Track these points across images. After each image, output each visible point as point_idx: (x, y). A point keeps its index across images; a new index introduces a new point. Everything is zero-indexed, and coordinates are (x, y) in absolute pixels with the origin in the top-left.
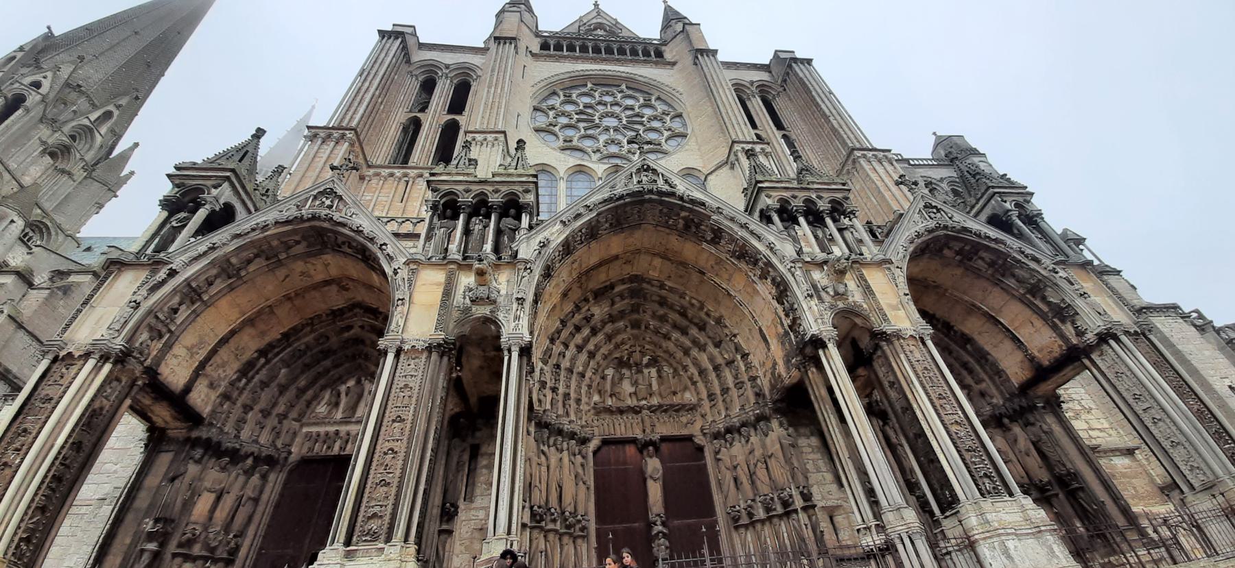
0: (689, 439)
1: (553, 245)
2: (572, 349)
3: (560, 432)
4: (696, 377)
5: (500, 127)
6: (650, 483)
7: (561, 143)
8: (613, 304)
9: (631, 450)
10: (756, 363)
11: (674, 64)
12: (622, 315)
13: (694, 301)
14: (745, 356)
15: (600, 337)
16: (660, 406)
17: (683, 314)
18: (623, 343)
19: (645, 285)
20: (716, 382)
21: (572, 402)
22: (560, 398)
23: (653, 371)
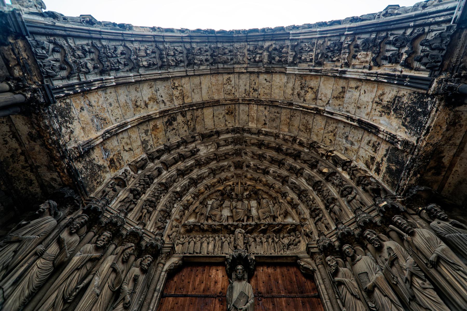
8: (219, 146)
12: (226, 156)
13: (287, 137)
15: (205, 170)
16: (257, 225)
18: (226, 179)
19: (245, 134)
20: (318, 200)
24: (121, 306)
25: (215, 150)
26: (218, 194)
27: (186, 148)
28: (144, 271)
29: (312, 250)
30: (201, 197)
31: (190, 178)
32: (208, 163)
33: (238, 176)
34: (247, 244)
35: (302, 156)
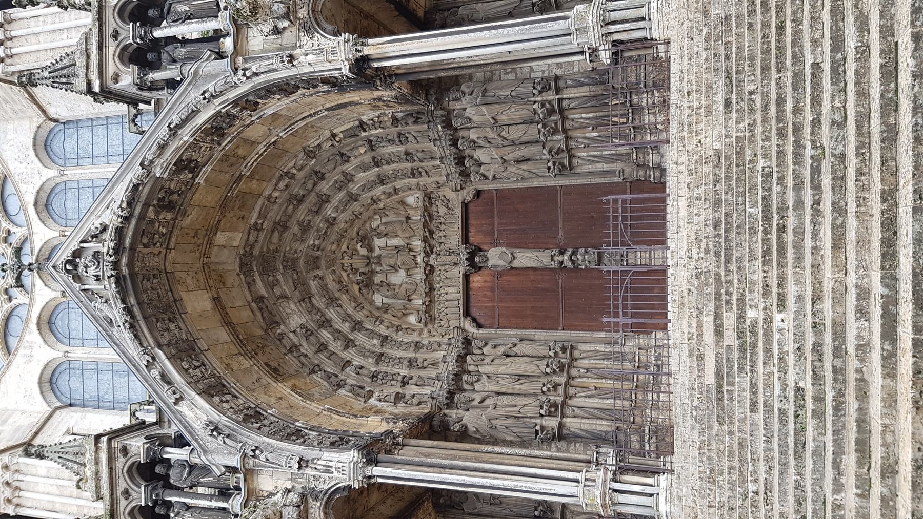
0: (465, 206)
1: (215, 416)
3: (457, 376)
4: (389, 188)
6: (516, 264)
9: (477, 280)
10: (373, 114)
12: (300, 284)
13: (281, 185)
14: (362, 126)
15: (332, 314)
16: (425, 240)
17: (301, 200)
19: (256, 252)
21: (420, 356)
22: (415, 373)
23: (378, 242)
24: (514, 349)
25: (291, 302)
26: (364, 291)
27: (301, 345)
28: (486, 344)
29: (459, 188)
30: (376, 313)
31: (352, 331)
32: (319, 310)
33: (332, 263)
34: (451, 252)
35: (323, 171)
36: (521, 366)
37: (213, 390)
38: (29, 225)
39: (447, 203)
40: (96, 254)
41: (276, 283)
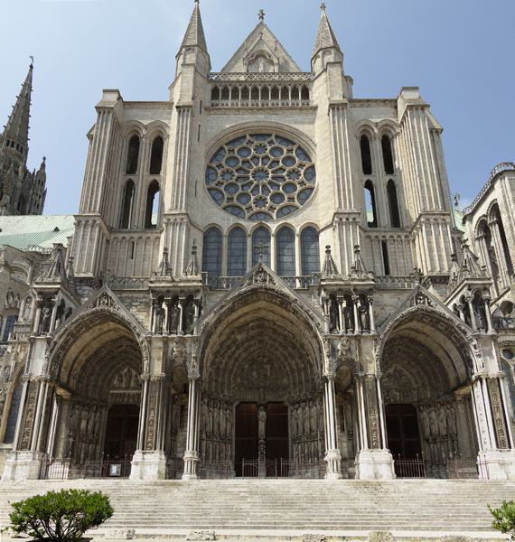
0: (282, 402)
2: (226, 357)
5: (184, 211)
6: (260, 422)
7: (225, 203)
9: (254, 406)
11: (316, 108)
14: (311, 366)
15: (241, 350)
17: (285, 340)
18: (254, 352)
21: (226, 385)
23: (268, 367)
34: (264, 396)
36: (223, 424)
37: (219, 321)
38: (277, 221)
39: (284, 395)
40: (265, 280)
41: (253, 329)
